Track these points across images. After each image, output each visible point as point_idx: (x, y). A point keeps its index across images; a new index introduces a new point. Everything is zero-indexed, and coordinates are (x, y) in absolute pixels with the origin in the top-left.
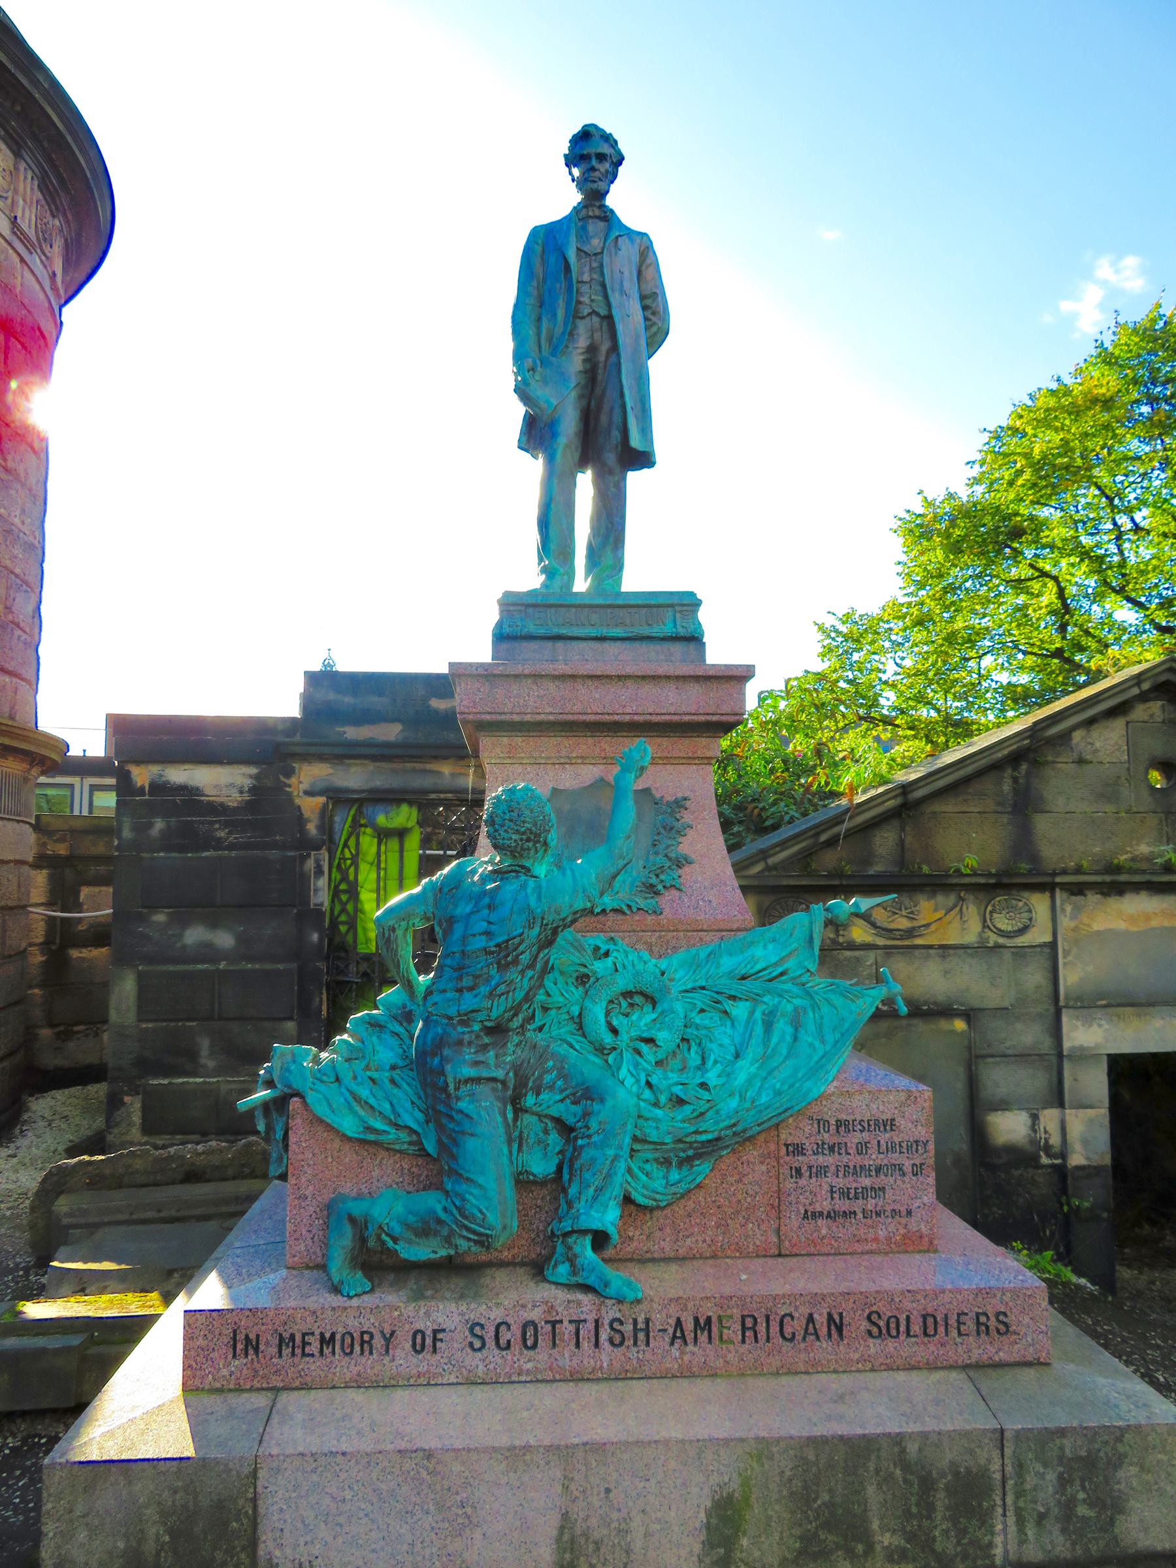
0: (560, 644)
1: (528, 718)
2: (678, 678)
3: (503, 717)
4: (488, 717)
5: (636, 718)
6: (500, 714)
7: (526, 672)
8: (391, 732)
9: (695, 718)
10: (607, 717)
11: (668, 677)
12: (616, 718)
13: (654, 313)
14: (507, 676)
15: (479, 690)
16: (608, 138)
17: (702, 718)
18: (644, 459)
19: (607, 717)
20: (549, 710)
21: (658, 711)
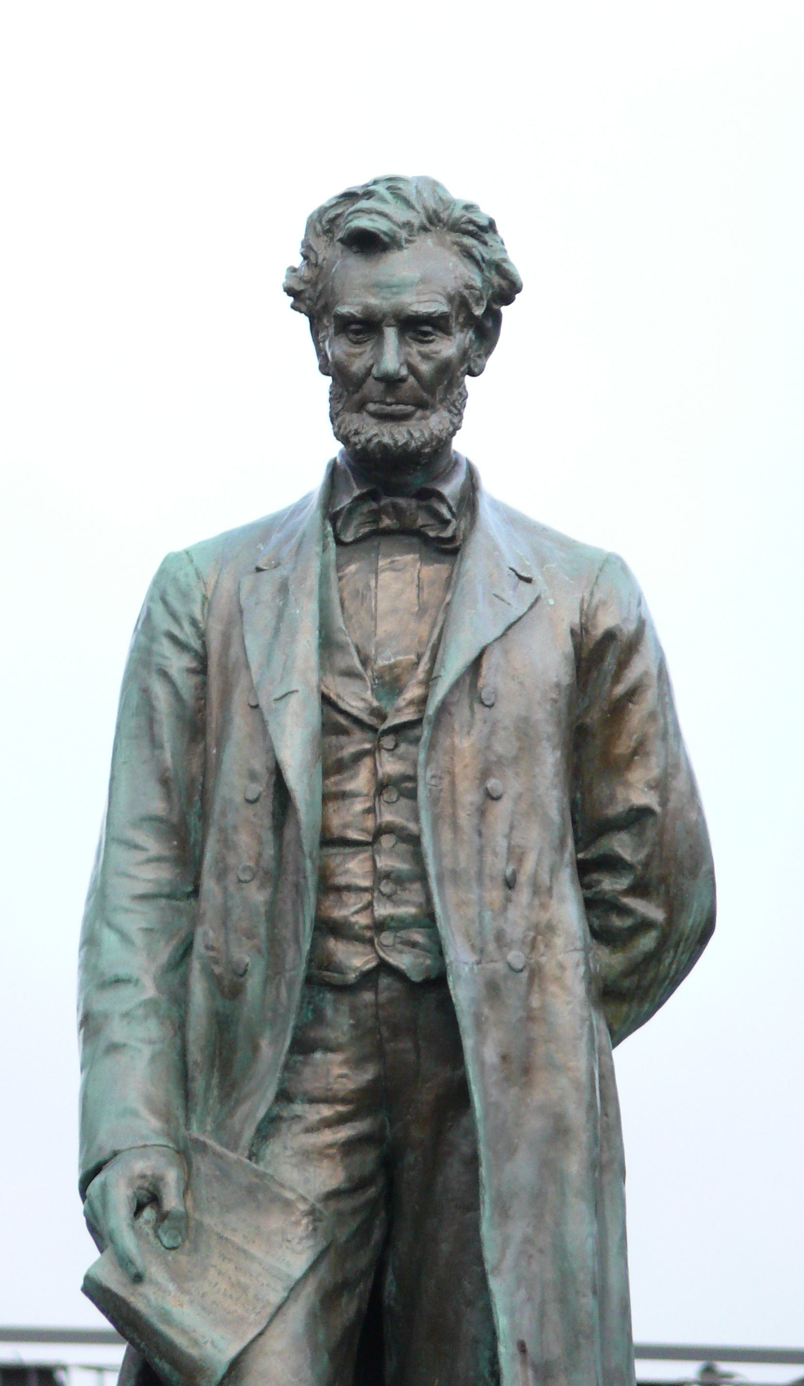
13: (640, 889)
16: (471, 232)
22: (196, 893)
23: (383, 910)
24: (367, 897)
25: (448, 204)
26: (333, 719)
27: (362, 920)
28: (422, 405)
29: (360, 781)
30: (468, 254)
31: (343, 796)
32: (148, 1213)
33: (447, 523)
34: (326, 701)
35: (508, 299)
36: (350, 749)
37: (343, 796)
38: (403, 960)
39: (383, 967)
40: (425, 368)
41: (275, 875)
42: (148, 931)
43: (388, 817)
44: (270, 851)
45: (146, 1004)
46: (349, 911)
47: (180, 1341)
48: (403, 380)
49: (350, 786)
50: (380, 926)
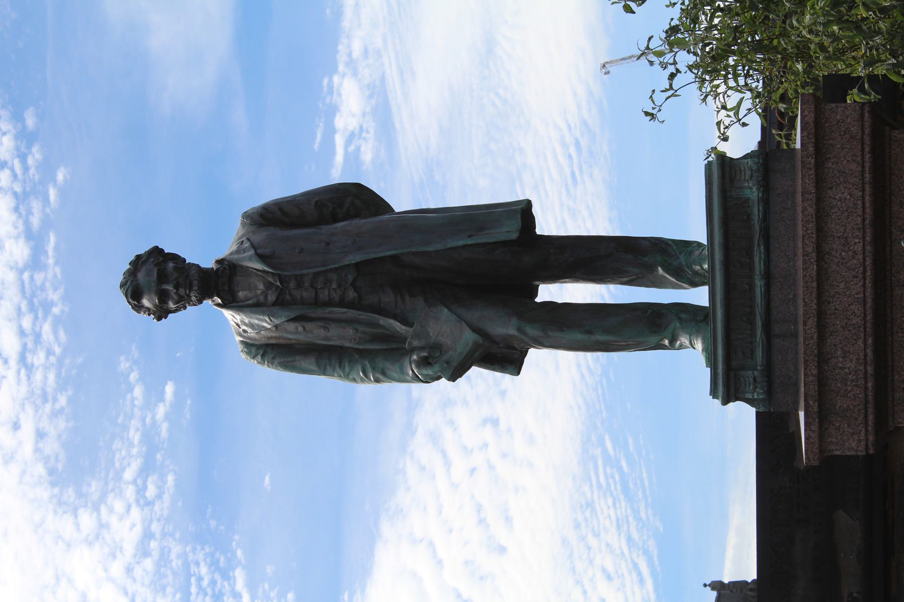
0: (777, 329)
1: (870, 369)
2: (818, 188)
3: (870, 398)
4: (871, 417)
5: (868, 239)
6: (866, 402)
7: (815, 372)
8: (849, 528)
9: (867, 165)
10: (869, 273)
11: (819, 200)
12: (868, 262)
14: (819, 395)
15: (838, 429)
16: (138, 263)
17: (867, 157)
18: (523, 212)
19: (869, 273)
20: (860, 342)
21: (860, 212)
22: (341, 347)
23: (334, 286)
24: (332, 291)
25: (129, 270)
26: (281, 303)
27: (339, 291)
28: (187, 277)
29: (297, 294)
30: (144, 262)
31: (302, 298)
32: (430, 360)
33: (225, 268)
34: (275, 304)
35: (162, 250)
36: (288, 297)
37: (302, 298)
38: (350, 278)
39: (353, 284)
40: (176, 275)
41: (326, 321)
42: (349, 362)
43: (307, 284)
44: (319, 323)
45: (370, 362)
46: (336, 297)
47: (467, 349)
48: (178, 283)
49: (299, 297)
50: (339, 286)
